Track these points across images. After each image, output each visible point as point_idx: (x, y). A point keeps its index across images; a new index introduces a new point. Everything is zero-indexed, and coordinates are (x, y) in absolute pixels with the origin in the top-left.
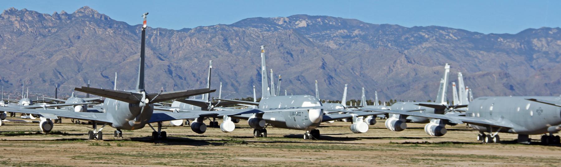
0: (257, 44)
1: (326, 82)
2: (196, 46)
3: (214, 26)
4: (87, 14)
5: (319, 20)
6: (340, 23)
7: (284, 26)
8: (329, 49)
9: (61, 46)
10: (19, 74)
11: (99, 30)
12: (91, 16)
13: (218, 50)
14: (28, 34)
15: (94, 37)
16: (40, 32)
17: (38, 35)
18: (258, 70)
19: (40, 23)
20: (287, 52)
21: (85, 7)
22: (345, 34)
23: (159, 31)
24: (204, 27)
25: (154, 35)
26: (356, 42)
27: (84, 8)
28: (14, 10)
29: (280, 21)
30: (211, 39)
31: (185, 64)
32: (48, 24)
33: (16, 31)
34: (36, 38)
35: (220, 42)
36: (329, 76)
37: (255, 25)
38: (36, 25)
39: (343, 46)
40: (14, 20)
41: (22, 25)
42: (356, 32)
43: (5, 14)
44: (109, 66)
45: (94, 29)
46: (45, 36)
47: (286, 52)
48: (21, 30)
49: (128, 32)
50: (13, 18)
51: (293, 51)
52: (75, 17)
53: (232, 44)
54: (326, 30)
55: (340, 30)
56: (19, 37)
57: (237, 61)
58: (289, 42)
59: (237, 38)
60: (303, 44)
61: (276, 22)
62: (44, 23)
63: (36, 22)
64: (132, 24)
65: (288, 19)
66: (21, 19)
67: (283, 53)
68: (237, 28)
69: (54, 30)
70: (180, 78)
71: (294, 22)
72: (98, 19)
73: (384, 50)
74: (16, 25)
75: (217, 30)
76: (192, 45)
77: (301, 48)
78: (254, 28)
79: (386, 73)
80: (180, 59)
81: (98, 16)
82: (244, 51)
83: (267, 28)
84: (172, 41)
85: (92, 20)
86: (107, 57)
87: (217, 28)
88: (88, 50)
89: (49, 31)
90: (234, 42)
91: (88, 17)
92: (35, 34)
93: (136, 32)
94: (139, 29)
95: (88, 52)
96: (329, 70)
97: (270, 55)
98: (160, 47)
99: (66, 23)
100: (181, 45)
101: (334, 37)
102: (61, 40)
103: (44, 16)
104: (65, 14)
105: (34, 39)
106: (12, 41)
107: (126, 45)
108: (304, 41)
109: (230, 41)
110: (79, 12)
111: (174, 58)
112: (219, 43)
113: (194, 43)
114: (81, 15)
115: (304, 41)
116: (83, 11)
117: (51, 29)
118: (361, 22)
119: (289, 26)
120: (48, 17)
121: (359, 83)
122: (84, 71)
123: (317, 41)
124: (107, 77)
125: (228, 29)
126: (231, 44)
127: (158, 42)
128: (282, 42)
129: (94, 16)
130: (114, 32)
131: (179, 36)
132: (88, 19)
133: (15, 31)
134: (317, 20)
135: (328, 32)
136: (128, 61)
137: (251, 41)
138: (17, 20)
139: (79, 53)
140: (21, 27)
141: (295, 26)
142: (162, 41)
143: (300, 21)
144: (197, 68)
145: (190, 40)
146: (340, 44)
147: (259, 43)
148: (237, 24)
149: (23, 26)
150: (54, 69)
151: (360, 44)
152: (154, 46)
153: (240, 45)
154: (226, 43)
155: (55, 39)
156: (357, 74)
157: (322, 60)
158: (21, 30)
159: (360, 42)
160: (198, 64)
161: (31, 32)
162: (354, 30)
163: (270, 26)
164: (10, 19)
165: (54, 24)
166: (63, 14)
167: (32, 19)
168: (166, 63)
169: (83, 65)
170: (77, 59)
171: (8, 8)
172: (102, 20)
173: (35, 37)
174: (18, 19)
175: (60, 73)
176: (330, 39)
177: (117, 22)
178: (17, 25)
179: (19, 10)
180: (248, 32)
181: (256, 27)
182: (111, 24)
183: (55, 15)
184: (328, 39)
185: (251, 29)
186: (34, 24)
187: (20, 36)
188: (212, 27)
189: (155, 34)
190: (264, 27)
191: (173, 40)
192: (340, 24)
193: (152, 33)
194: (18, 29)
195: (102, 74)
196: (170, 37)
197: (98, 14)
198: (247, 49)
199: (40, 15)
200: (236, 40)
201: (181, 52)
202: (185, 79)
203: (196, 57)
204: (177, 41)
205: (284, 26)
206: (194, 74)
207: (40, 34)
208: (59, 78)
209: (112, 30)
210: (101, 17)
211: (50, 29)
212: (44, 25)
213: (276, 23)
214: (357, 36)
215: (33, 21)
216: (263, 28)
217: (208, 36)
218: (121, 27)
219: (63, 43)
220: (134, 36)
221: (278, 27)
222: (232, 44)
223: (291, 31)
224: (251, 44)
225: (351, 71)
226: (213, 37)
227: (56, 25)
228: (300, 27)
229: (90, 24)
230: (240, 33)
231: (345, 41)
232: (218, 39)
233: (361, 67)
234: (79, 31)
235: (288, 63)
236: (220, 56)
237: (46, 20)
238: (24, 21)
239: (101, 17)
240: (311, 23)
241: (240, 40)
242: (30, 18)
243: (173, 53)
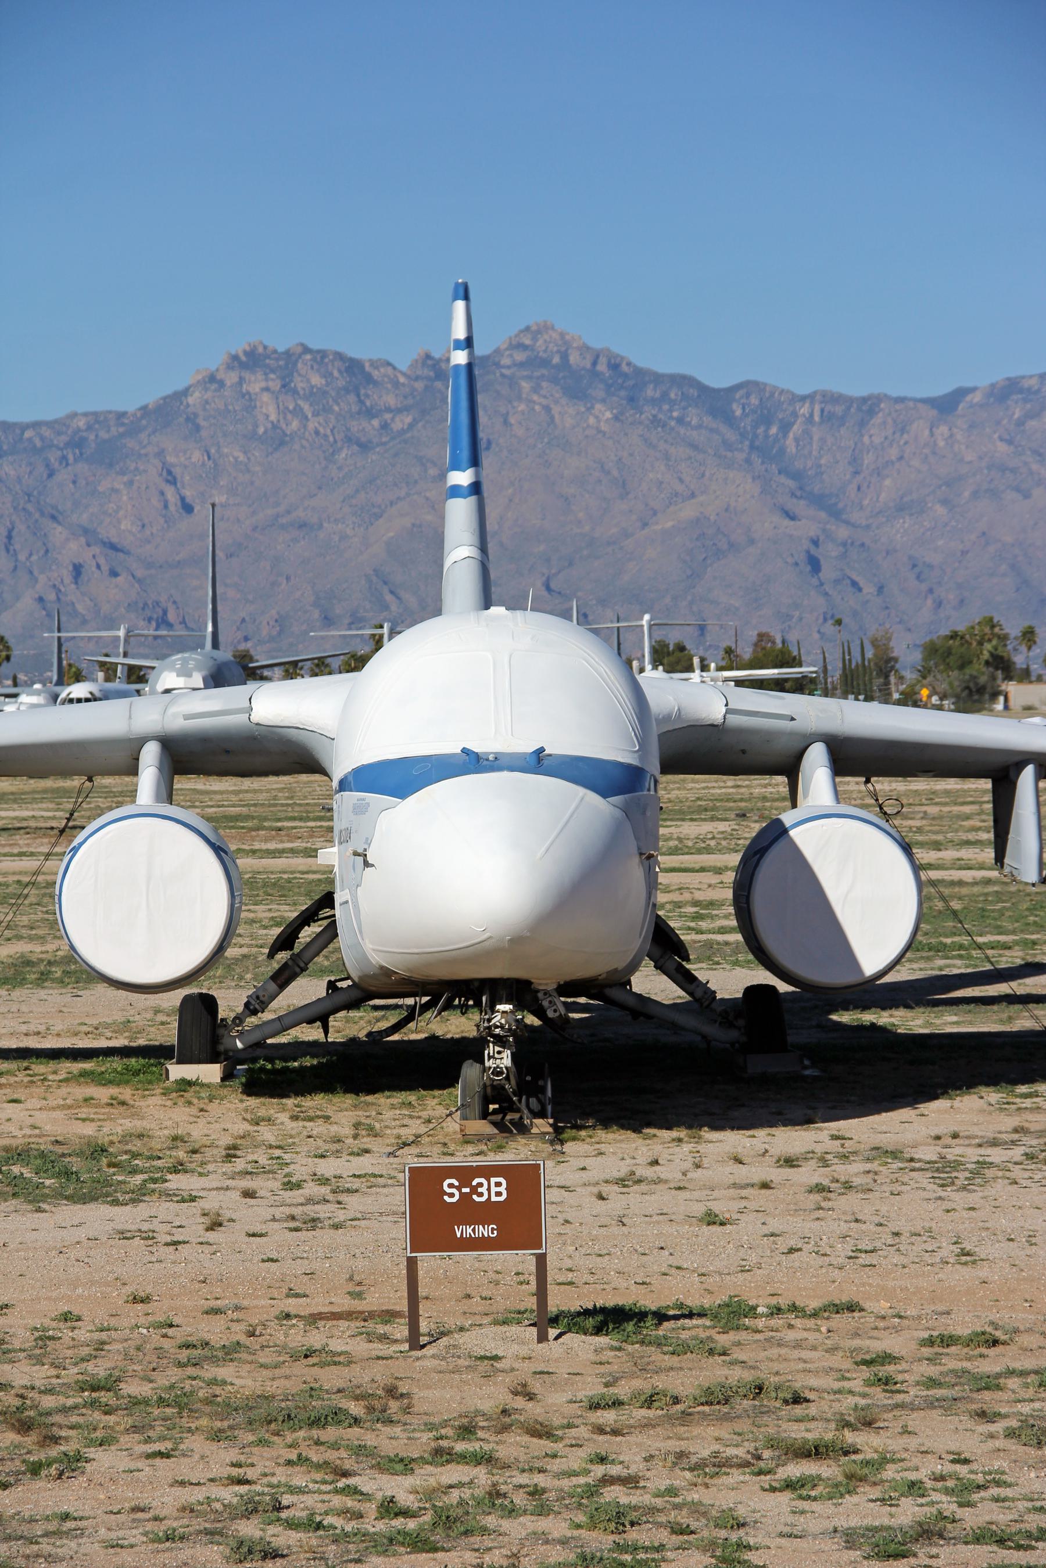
4: (541, 354)
9: (416, 482)
10: (250, 597)
12: (556, 360)
13: (1035, 467)
14: (304, 442)
15: (546, 440)
16: (348, 430)
17: (339, 444)
19: (352, 398)
21: (537, 324)
24: (1023, 377)
25: (799, 421)
27: (534, 328)
28: (260, 350)
30: (1020, 423)
32: (381, 397)
33: (265, 432)
34: (333, 454)
38: (338, 404)
40: (257, 390)
41: (287, 408)
43: (229, 367)
45: (547, 409)
46: (365, 447)
48: (284, 426)
50: (255, 383)
52: (498, 365)
56: (272, 453)
62: (367, 396)
64: (717, 379)
66: (284, 386)
74: (264, 410)
76: (934, 453)
80: (880, 512)
81: (584, 358)
84: (866, 439)
85: (561, 375)
86: (581, 515)
88: (510, 491)
91: (545, 363)
92: (331, 439)
93: (733, 412)
94: (744, 401)
95: (511, 500)
98: (820, 466)
100: (893, 453)
103: (367, 368)
105: (325, 459)
106: (248, 471)
111: (861, 508)
113: (941, 444)
116: (527, 342)
120: (382, 370)
129: (568, 361)
130: (616, 418)
131: (894, 421)
132: (545, 371)
133: (261, 430)
136: (658, 527)
138: (267, 389)
140: (281, 416)
144: (940, 543)
145: (927, 432)
149: (290, 412)
150: (372, 572)
152: (798, 465)
155: (396, 455)
158: (281, 429)
161: (317, 433)
164: (245, 386)
167: (323, 381)
171: (238, 347)
172: (594, 373)
173: (331, 450)
174: (271, 384)
177: (658, 379)
178: (268, 408)
179: (281, 349)
183: (424, 364)
186: (331, 402)
187: (276, 449)
189: (804, 415)
191: (871, 436)
193: (795, 414)
194: (272, 422)
196: (862, 424)
197: (585, 349)
199: (353, 366)
201: (888, 482)
203: (945, 502)
204: (886, 438)
207: (349, 440)
210: (595, 363)
211: (388, 416)
212: (368, 403)
215: (328, 389)
217: (1013, 414)
218: (672, 396)
219: (426, 471)
220: (724, 429)
229: (536, 389)
236: (1036, 492)
237: (376, 383)
238: (295, 392)
239: (595, 363)
242: (316, 380)
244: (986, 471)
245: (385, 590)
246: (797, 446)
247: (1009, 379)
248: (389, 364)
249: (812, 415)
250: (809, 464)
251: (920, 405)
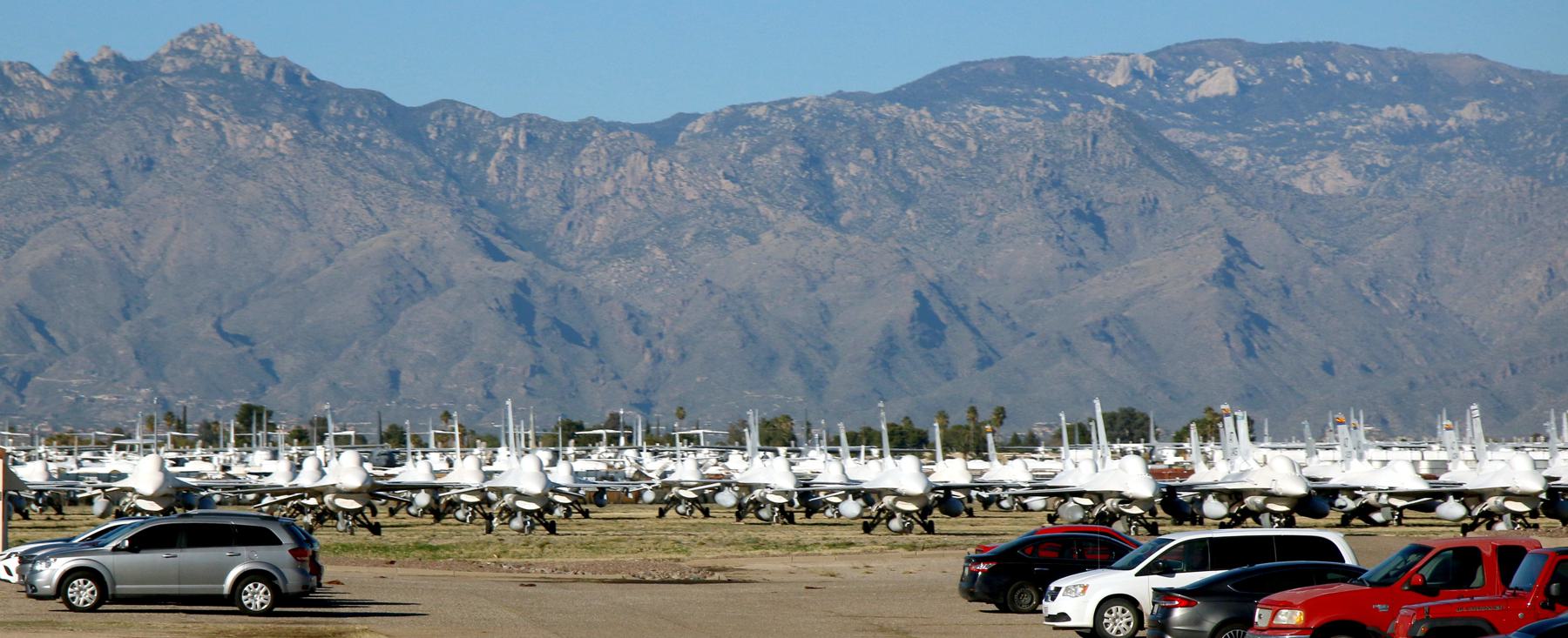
0: (947, 178)
1: (1233, 344)
2: (671, 193)
4: (207, 62)
5: (1298, 61)
6: (1395, 72)
7: (1133, 92)
8: (1283, 193)
9: (65, 205)
11: (240, 130)
12: (225, 69)
13: (762, 209)
15: (215, 161)
18: (926, 294)
20: (1078, 214)
21: (204, 28)
22: (1409, 123)
23: (527, 127)
24: (750, 105)
25: (503, 146)
26: (1447, 157)
27: (200, 31)
29: (1113, 70)
30: (747, 159)
31: (611, 277)
32: (22, 105)
35: (786, 173)
36: (1247, 317)
37: (995, 90)
39: (1386, 178)
42: (1470, 113)
44: (262, 290)
45: (217, 126)
47: (1072, 212)
49: (388, 137)
51: (1106, 206)
52: (157, 72)
53: (841, 182)
54: (1327, 107)
55: (1393, 105)
57: (838, 256)
58: (1092, 164)
59: (867, 154)
60: (1154, 173)
61: (1097, 74)
65: (1153, 62)
67: (1055, 215)
69: (47, 133)
70: (571, 336)
71: (1181, 73)
72: (258, 80)
73: (1532, 191)
75: (807, 118)
76: (653, 190)
77: (1143, 192)
78: (989, 108)
79: (1534, 300)
80: (593, 254)
83: (1052, 106)
84: (577, 171)
85: (231, 86)
87: (807, 108)
89: (27, 139)
90: (853, 169)
91: (212, 72)
93: (428, 134)
95: (177, 229)
96: (1256, 289)
97: (995, 225)
98: (525, 199)
99: (99, 103)
100: (608, 187)
101: (1359, 136)
102: (68, 178)
104: (112, 59)
107: (344, 192)
108: (1163, 160)
109: (832, 169)
110: (178, 51)
111: (572, 247)
112: (785, 178)
113: (661, 179)
114: (182, 63)
115: (1163, 160)
116: (192, 47)
118: (1495, 68)
119: (1154, 93)
121: (1396, 347)
122: (150, 313)
123: (1271, 158)
124: (245, 340)
125: (854, 115)
126: (839, 182)
127: (520, 177)
128: (1062, 166)
129: (240, 70)
130: (298, 139)
131: (607, 150)
132: (212, 82)
134: (1289, 61)
135: (1335, 115)
137: (925, 162)
141: (1182, 95)
142: (536, 171)
143: (1209, 69)
144: (660, 290)
145: (645, 166)
146: (1368, 168)
147: (959, 172)
148: (911, 95)
150: (14, 307)
151: (1464, 167)
153: (875, 184)
154: (816, 176)
156: (1395, 304)
157: (1226, 246)
159: (1465, 156)
160: (668, 274)
162: (1461, 105)
163: (1064, 94)
165: (51, 106)
166: (102, 63)
168: (511, 271)
169: (147, 288)
170: (127, 260)
172: (273, 87)
175: (40, 326)
176: (1331, 148)
177: (342, 94)
180: (917, 126)
181: (1002, 101)
182: (314, 102)
183: (70, 68)
184: (1320, 148)
185: (974, 111)
188: (784, 108)
189: (507, 141)
190: (1039, 102)
191: (582, 167)
192: (1395, 79)
193: (497, 140)
195: (218, 327)
196: (573, 153)
197: (259, 58)
198: (906, 200)
200: (859, 162)
201: (601, 220)
202: (595, 341)
203: (664, 245)
204: (599, 170)
205: (1133, 92)
206: (634, 320)
208: (33, 348)
209: (290, 128)
210: (270, 73)
211: (30, 128)
213: (1094, 80)
214: (1463, 131)
216: (1033, 105)
217: (740, 148)
218: (359, 114)
219: (76, 191)
220: (415, 152)
221: (1101, 98)
222: (841, 182)
223: (1105, 117)
224: (924, 175)
225: (1367, 291)
226: (758, 150)
227: (57, 111)
228: (1205, 100)
229: (204, 103)
230: (879, 131)
231: (1396, 156)
232: (777, 161)
233: (1425, 275)
234: (150, 135)
235: (1077, 259)
236: (766, 237)
237: (16, 88)
239: (270, 73)
240: (1259, 75)
243: (570, 225)
244: (709, 212)
245: (30, 327)
246: (500, 175)
247: (733, 107)
248: (32, 68)
249: (516, 140)
250: (513, 196)
251: (636, 135)
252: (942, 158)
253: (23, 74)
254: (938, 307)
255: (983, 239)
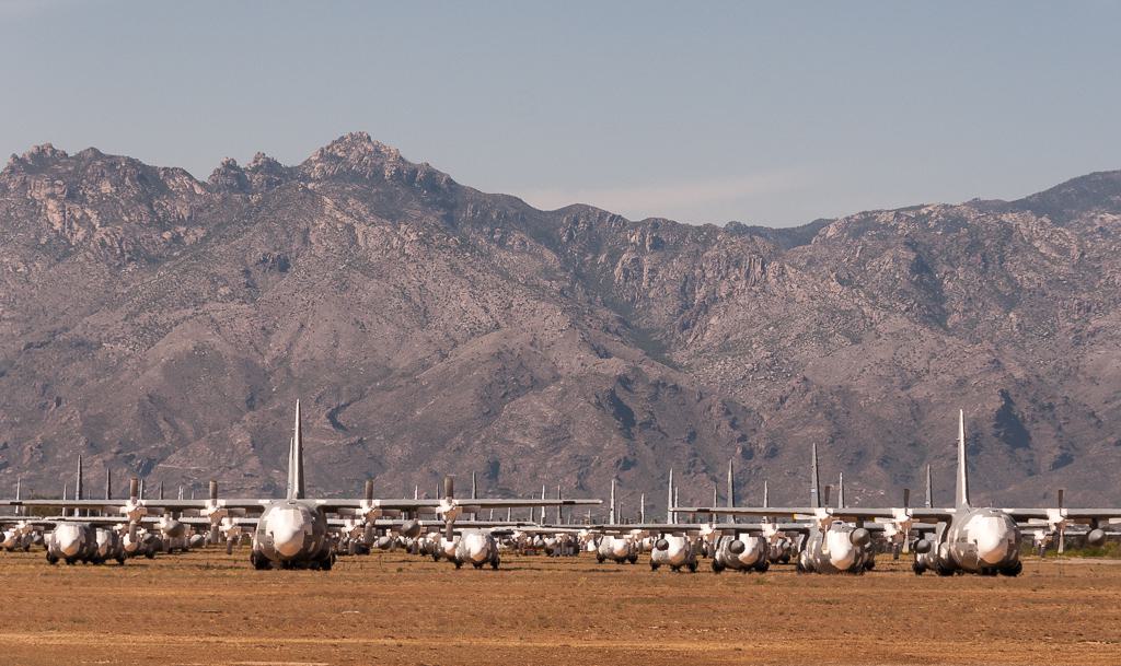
3: (923, 206)
14: (88, 253)
16: (137, 242)
18: (1012, 393)
19: (144, 208)
38: (129, 215)
41: (73, 217)
45: (350, 228)
46: (154, 261)
52: (306, 178)
63: (129, 202)
66: (71, 196)
68: (1016, 215)
82: (995, 313)
87: (933, 215)
89: (177, 239)
99: (245, 206)
100: (723, 290)
109: (942, 269)
110: (326, 155)
112: (896, 281)
117: (185, 233)
126: (948, 285)
130: (421, 241)
133: (43, 241)
138: (52, 196)
139: (263, 329)
148: (1038, 205)
154: (926, 279)
155: (186, 271)
161: (103, 244)
166: (255, 170)
168: (614, 366)
171: (25, 149)
180: (1024, 232)
185: (1101, 219)
189: (635, 243)
193: (626, 242)
198: (1010, 303)
211: (182, 229)
241: (986, 267)
247: (865, 213)
252: (1047, 263)
253: (177, 180)
254: (1023, 408)
255: (1078, 341)
